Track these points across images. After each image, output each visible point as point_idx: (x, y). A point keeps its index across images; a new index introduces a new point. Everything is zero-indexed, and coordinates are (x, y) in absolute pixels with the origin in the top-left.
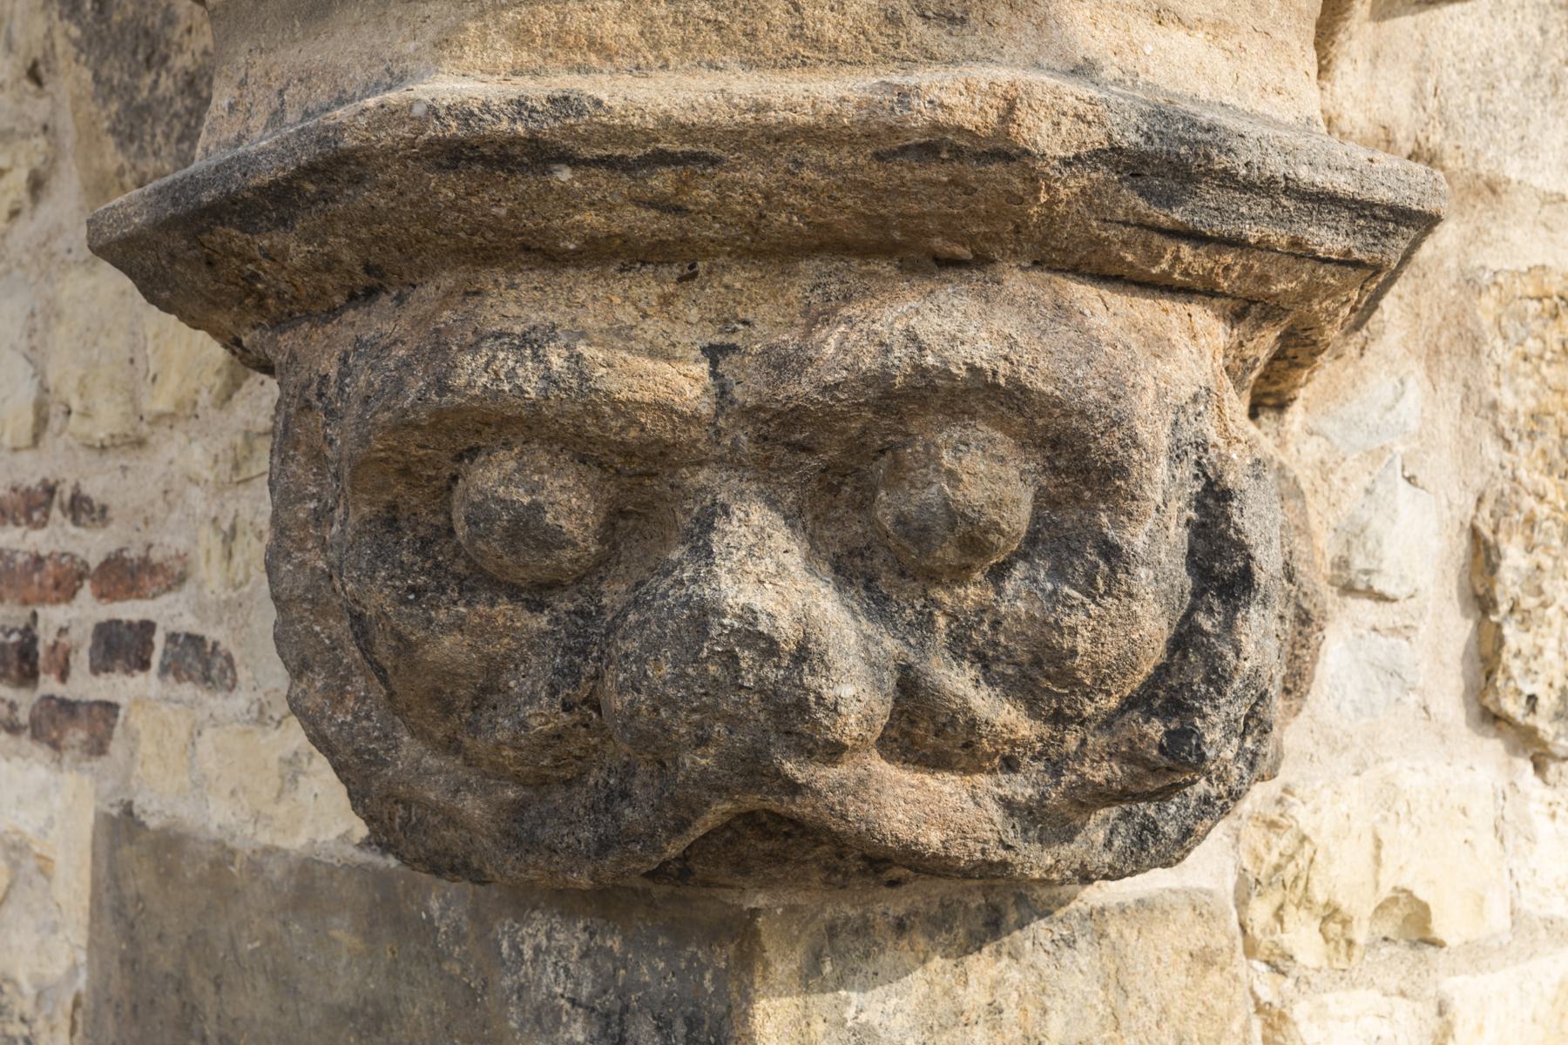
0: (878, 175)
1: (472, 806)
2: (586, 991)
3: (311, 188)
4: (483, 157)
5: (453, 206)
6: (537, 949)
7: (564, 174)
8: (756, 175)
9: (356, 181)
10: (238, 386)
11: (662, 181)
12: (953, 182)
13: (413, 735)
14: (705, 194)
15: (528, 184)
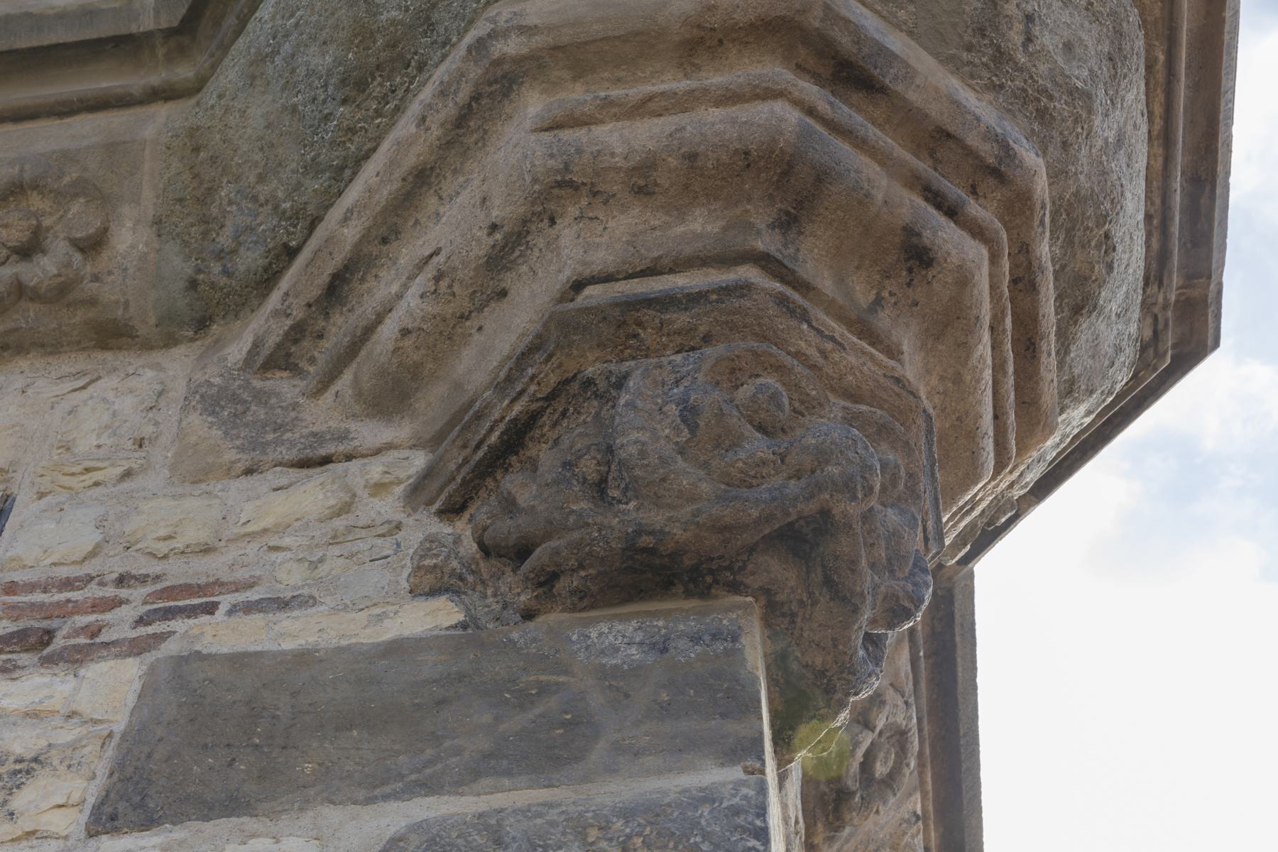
0: (882, 380)
1: (705, 487)
2: (637, 640)
3: (714, 297)
4: (788, 308)
5: (769, 317)
6: (601, 634)
7: (805, 326)
8: (852, 359)
9: (742, 296)
10: (339, 515)
11: (829, 346)
12: (898, 395)
13: (685, 460)
14: (836, 356)
15: (793, 323)
